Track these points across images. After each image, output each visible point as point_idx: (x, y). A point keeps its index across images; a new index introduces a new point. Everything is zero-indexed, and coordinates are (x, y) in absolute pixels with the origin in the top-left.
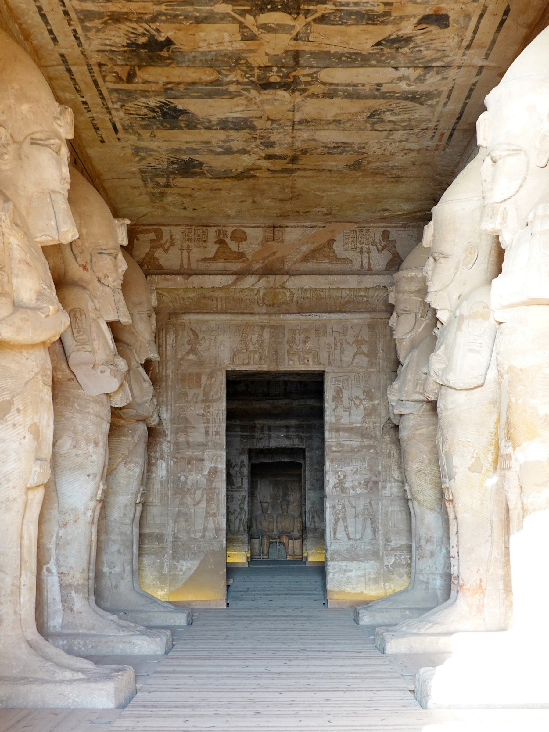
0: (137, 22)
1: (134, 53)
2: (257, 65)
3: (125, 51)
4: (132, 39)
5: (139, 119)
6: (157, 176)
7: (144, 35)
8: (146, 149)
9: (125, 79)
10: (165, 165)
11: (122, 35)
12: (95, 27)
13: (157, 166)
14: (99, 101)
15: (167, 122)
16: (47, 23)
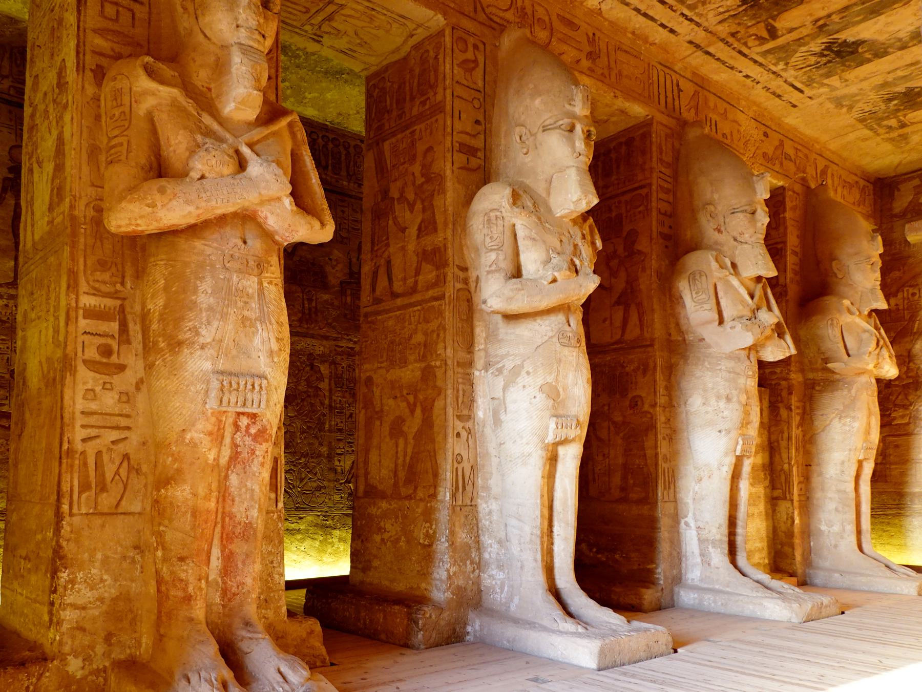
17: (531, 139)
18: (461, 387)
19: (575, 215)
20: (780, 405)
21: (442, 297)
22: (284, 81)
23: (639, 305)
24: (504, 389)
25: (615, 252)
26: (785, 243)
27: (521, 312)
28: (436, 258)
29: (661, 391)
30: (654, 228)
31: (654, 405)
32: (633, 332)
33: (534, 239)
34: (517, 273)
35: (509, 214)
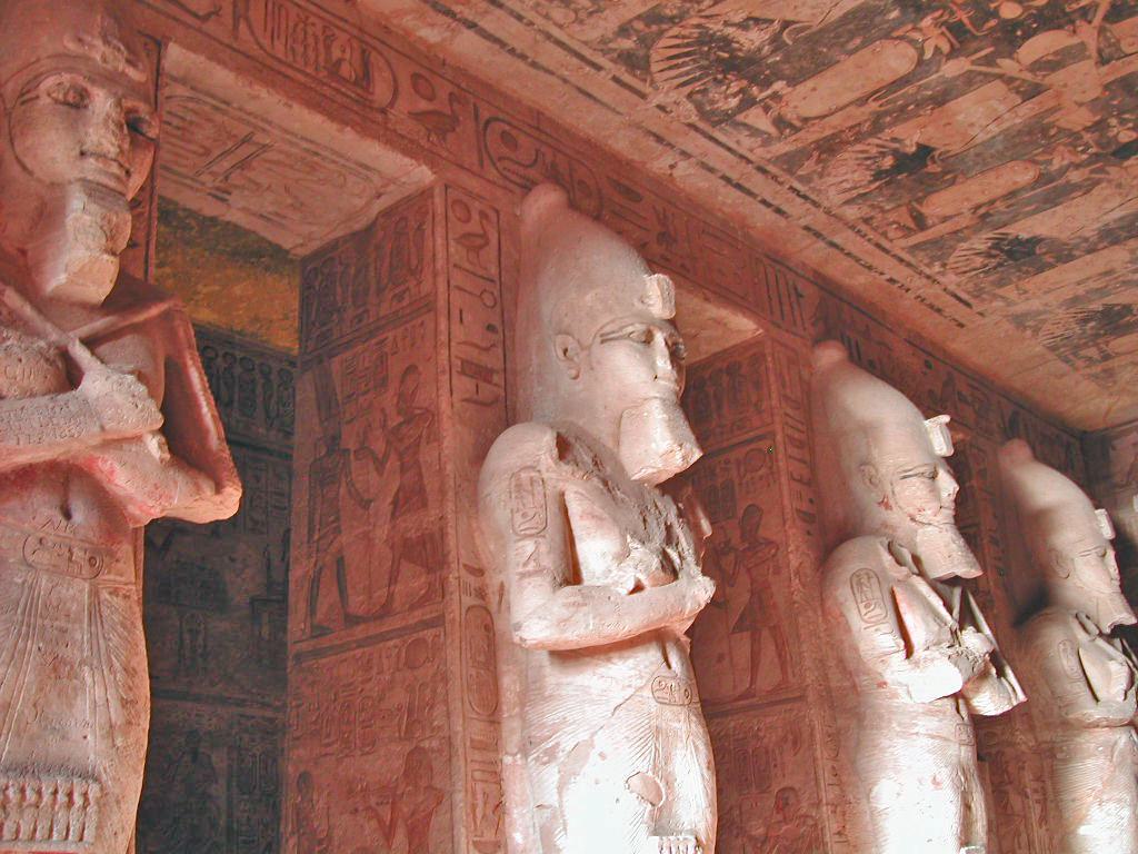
0: (857, 141)
1: (893, 185)
2: (1080, 128)
3: (879, 188)
4: (873, 167)
5: (982, 276)
6: (1078, 347)
7: (883, 154)
8: (1025, 315)
9: (912, 226)
10: (1078, 330)
11: (856, 167)
12: (815, 171)
13: (1067, 333)
14: (908, 271)
15: (1024, 264)
16: (749, 193)
17: (583, 355)
18: (479, 787)
19: (664, 477)
20: (1009, 788)
21: (438, 621)
22: (160, 265)
23: (775, 629)
24: (561, 788)
25: (727, 543)
26: (977, 525)
27: (584, 644)
28: (428, 552)
29: (826, 777)
30: (786, 502)
31: (818, 804)
32: (769, 676)
33: (601, 519)
34: (571, 574)
35: (554, 475)
